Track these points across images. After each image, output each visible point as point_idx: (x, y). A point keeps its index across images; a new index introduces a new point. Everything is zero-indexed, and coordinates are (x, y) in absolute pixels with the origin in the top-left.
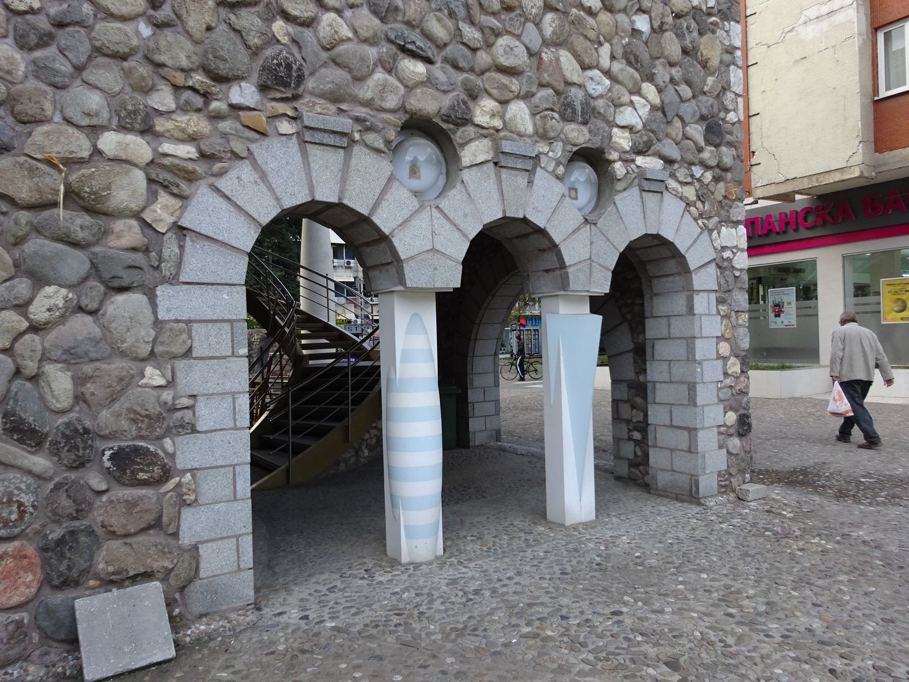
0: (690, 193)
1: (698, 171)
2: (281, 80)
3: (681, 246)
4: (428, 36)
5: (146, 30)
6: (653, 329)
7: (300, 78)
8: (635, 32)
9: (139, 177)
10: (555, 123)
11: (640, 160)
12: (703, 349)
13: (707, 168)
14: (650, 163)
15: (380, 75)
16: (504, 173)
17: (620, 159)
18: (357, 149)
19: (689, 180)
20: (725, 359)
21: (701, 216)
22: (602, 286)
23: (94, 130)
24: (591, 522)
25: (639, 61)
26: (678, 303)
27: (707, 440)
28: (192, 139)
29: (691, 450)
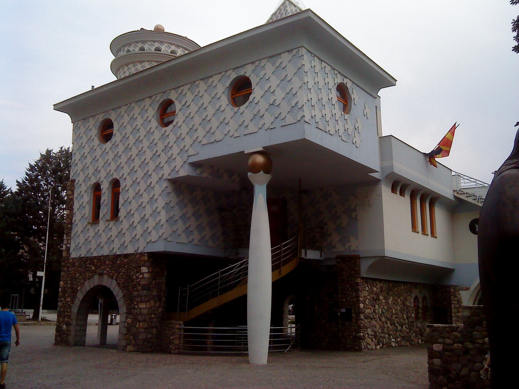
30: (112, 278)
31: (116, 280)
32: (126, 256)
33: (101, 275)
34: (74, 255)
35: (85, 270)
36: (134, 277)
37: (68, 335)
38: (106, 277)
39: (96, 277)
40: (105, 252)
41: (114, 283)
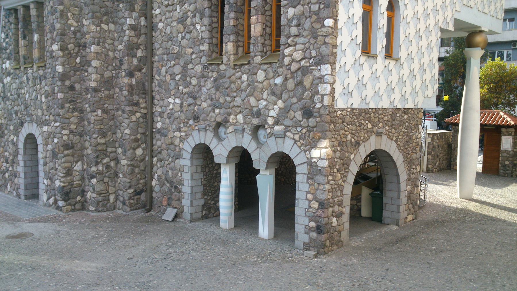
0: (297, 137)
1: (299, 129)
2: (196, 118)
5: (179, 113)
7: (198, 117)
9: (178, 139)
16: (237, 134)
17: (269, 127)
18: (208, 131)
19: (297, 132)
20: (310, 201)
21: (302, 145)
24: (266, 240)
28: (185, 132)
30: (392, 140)
31: (396, 141)
32: (406, 111)
33: (379, 134)
34: (340, 103)
35: (358, 128)
36: (414, 137)
37: (339, 232)
38: (384, 137)
39: (373, 138)
40: (385, 104)
41: (394, 144)
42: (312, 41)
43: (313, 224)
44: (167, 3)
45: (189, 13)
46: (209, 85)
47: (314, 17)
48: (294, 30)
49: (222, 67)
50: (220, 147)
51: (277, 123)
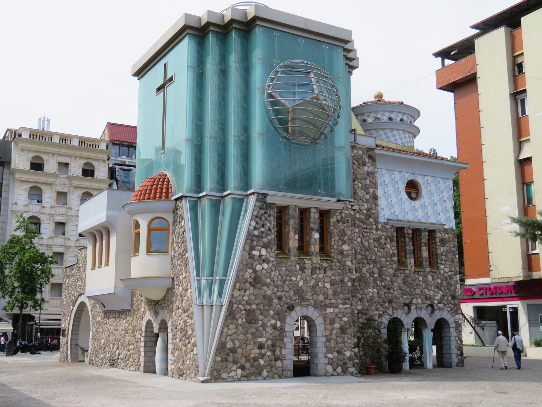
0: (449, 309)
1: (450, 305)
2: (390, 302)
3: (447, 319)
4: (406, 291)
6: (443, 334)
8: (438, 283)
10: (425, 301)
11: (439, 305)
12: (452, 339)
13: (452, 304)
14: (441, 305)
15: (401, 299)
22: (433, 327)
23: (374, 311)
25: (438, 287)
26: (448, 330)
27: (454, 356)
29: (451, 358)
42: (452, 264)
43: (459, 352)
44: (365, 226)
45: (383, 237)
46: (400, 281)
47: (452, 254)
48: (444, 258)
49: (407, 272)
50: (407, 318)
51: (439, 303)
